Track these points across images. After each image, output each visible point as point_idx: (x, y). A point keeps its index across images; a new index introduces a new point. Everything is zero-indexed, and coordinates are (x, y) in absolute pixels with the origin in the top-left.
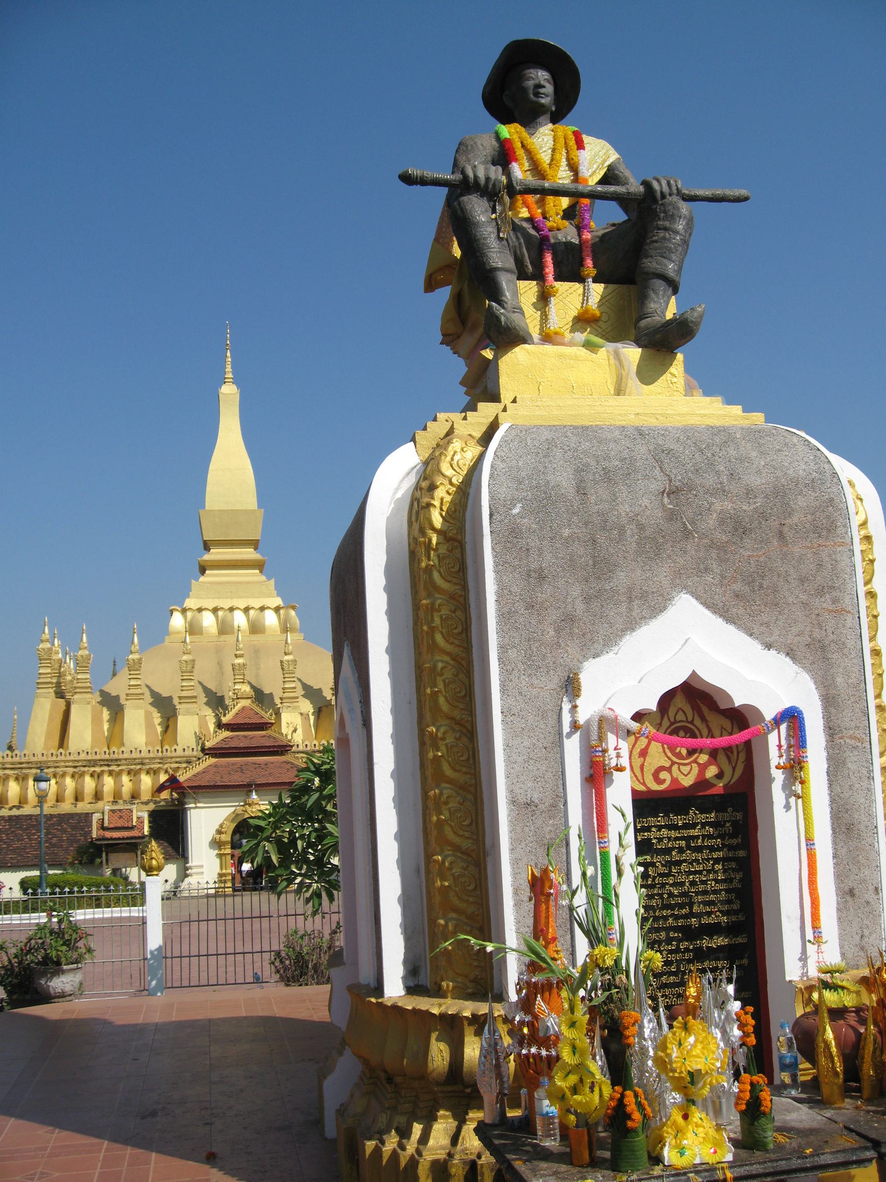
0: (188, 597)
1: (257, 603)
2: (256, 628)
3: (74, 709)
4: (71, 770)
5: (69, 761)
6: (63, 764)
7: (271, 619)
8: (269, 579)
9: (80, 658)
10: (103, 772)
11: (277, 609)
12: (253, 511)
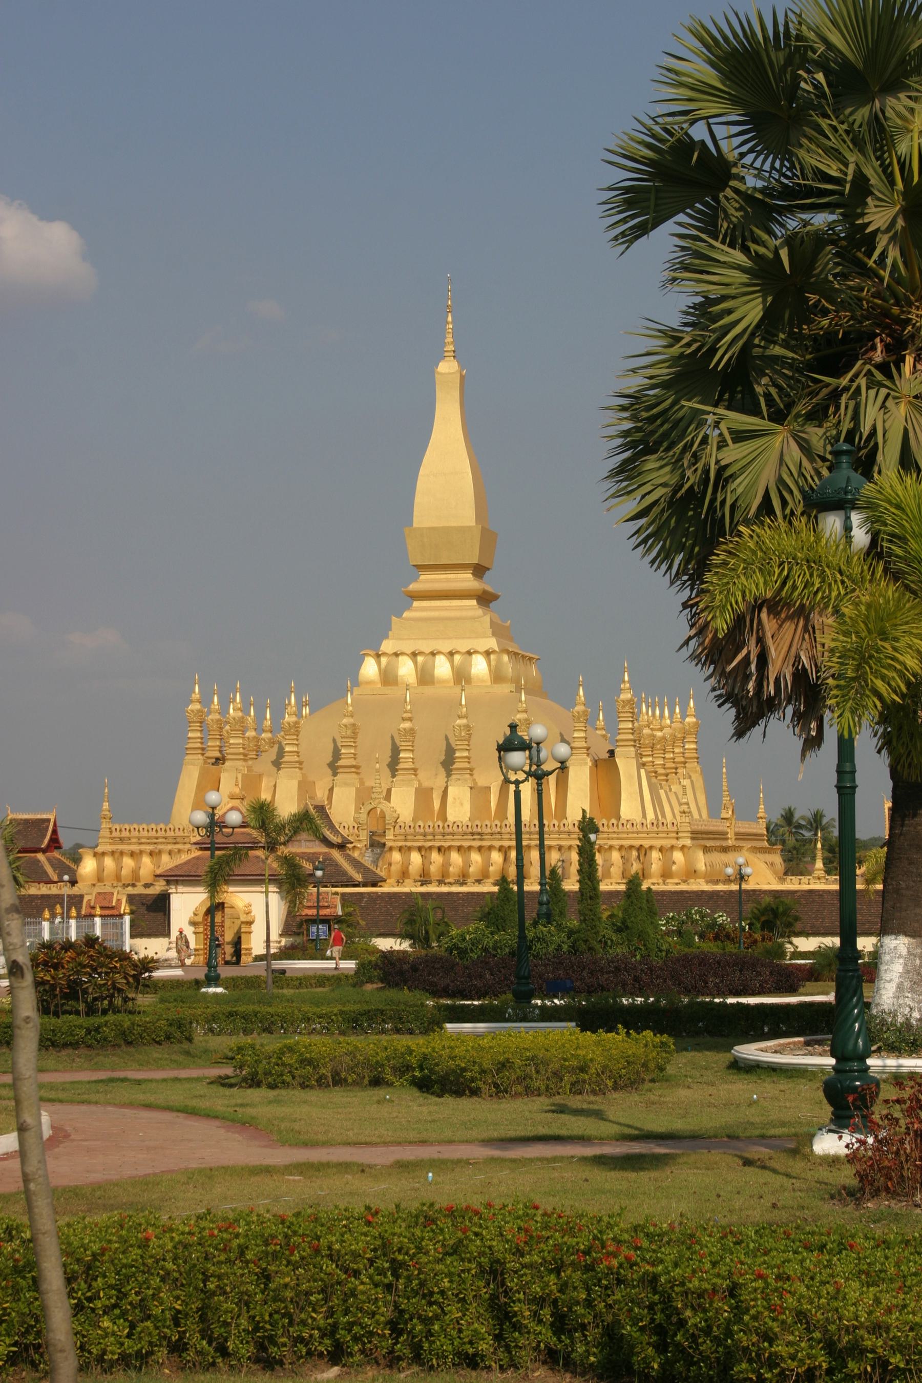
0: (387, 637)
1: (463, 645)
2: (461, 676)
7: (479, 667)
11: (488, 654)
12: (470, 528)
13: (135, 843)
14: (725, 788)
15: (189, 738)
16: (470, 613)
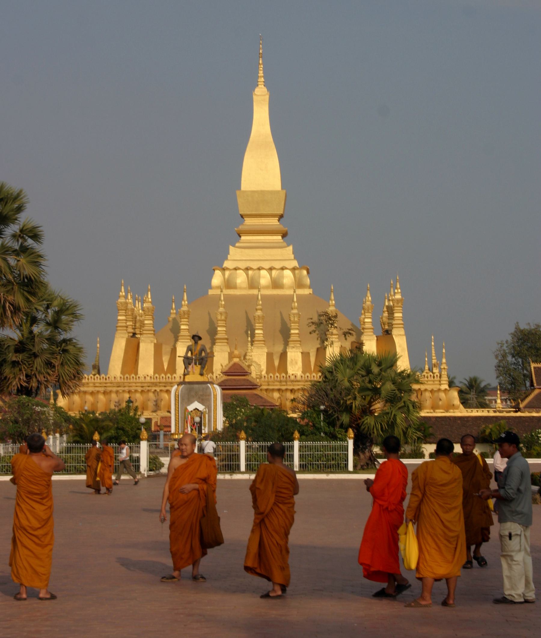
2: (276, 284)
3: (142, 345)
4: (140, 389)
5: (138, 383)
6: (134, 384)
7: (288, 277)
8: (288, 245)
9: (146, 309)
10: (161, 391)
11: (293, 269)
12: (278, 192)
13: (92, 387)
14: (434, 355)
15: (118, 320)
16: (280, 245)
